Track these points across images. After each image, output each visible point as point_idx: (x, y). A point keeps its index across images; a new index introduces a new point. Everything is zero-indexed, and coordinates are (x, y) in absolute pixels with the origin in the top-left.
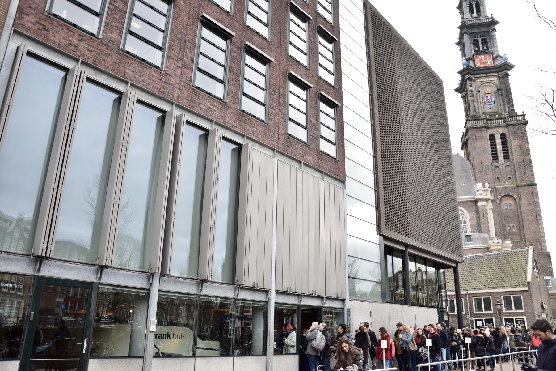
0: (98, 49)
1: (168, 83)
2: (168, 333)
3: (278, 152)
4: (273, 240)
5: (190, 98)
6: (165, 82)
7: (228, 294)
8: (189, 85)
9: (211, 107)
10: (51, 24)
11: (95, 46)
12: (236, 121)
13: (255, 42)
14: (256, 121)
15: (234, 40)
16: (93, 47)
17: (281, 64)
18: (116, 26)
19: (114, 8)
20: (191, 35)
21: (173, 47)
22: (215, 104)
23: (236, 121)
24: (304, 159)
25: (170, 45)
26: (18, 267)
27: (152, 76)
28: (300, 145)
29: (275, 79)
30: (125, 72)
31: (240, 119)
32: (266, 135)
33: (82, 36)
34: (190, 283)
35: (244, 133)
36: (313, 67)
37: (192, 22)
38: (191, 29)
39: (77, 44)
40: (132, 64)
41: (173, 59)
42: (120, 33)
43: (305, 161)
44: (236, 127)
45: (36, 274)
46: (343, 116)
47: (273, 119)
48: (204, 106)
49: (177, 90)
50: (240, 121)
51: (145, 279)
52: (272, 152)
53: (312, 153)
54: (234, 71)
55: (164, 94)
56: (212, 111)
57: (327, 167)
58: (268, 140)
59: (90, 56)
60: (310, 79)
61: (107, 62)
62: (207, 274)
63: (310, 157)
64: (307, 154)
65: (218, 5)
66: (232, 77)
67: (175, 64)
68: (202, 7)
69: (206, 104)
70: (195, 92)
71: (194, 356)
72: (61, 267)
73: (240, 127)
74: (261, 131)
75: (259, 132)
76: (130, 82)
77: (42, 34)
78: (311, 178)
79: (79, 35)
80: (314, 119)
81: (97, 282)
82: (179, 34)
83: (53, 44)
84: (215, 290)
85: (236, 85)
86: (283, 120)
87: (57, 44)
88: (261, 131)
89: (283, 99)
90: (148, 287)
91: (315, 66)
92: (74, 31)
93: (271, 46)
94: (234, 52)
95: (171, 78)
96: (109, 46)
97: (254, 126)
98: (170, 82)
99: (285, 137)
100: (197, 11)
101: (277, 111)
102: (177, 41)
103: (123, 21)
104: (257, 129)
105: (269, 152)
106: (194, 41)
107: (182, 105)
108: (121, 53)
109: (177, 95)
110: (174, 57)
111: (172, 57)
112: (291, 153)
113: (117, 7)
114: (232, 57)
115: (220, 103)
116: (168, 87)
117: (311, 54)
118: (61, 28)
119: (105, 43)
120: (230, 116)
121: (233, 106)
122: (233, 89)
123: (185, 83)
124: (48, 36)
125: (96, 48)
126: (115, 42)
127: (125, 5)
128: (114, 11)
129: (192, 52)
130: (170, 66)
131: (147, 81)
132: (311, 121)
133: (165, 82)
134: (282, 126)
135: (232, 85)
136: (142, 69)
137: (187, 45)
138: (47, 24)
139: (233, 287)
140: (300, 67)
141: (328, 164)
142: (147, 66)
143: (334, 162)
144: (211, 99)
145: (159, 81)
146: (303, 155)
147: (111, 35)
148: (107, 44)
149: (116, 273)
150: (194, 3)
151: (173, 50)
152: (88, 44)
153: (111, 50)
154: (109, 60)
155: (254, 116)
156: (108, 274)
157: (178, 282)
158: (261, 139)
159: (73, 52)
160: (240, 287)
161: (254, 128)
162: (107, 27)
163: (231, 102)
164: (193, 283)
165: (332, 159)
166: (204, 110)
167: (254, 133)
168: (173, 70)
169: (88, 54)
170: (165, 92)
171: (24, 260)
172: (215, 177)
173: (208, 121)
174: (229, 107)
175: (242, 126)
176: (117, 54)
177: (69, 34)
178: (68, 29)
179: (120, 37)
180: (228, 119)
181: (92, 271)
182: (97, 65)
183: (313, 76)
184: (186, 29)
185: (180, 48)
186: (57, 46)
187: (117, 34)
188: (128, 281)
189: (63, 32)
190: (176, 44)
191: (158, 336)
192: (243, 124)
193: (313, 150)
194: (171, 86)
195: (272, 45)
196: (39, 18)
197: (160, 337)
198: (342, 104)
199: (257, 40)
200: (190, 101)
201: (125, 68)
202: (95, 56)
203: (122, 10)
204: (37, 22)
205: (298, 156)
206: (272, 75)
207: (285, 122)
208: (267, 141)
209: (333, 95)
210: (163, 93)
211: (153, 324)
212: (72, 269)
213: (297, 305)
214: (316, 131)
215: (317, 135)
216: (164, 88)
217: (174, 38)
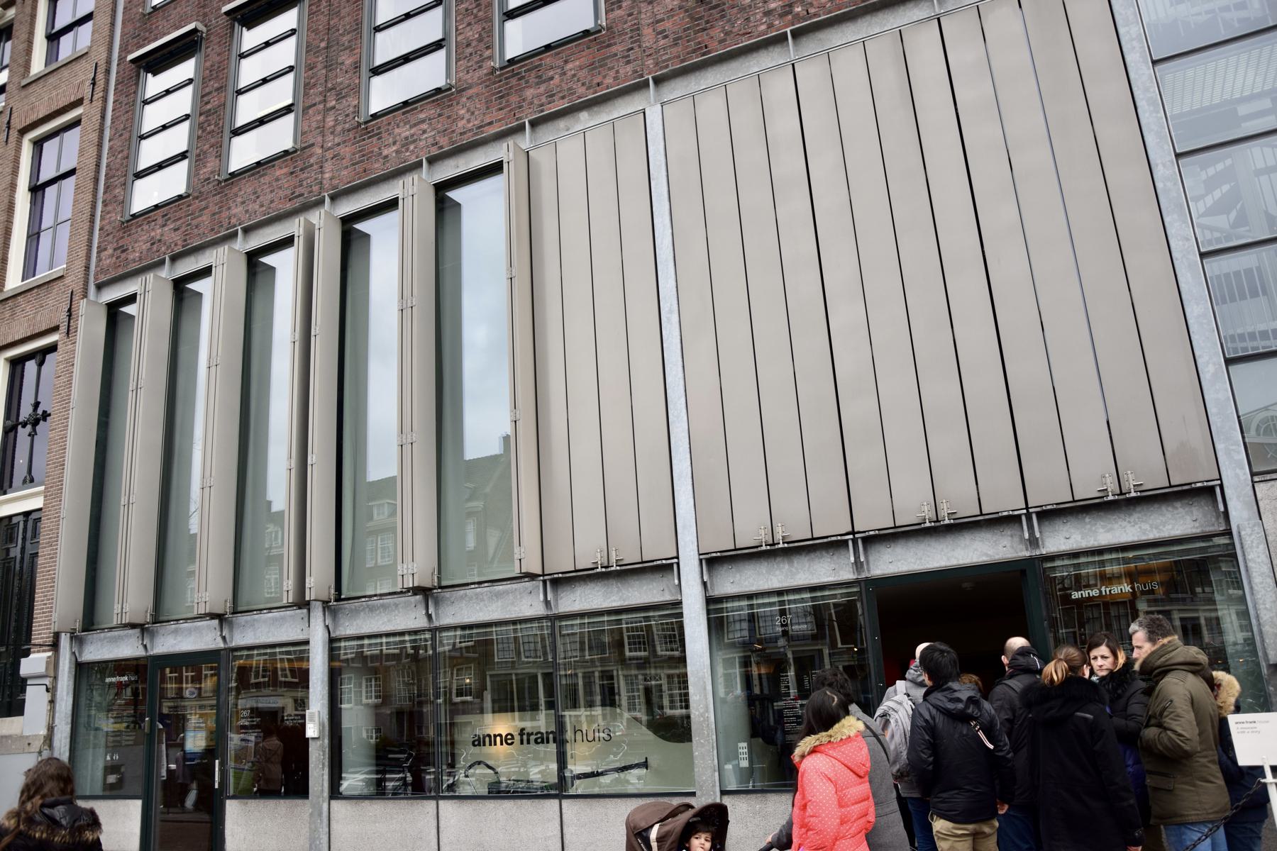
16: (180, 218)
23: (488, 108)
31: (500, 92)
35: (517, 120)
44: (491, 123)
58: (612, 73)
73: (501, 114)
74: (581, 68)
75: (574, 75)
88: (581, 68)
111: (314, 102)
133: (301, 170)
147: (205, 170)
149: (254, 620)
161: (552, 78)
180: (461, 124)
191: (533, 738)
205: (763, 27)
211: (312, 720)
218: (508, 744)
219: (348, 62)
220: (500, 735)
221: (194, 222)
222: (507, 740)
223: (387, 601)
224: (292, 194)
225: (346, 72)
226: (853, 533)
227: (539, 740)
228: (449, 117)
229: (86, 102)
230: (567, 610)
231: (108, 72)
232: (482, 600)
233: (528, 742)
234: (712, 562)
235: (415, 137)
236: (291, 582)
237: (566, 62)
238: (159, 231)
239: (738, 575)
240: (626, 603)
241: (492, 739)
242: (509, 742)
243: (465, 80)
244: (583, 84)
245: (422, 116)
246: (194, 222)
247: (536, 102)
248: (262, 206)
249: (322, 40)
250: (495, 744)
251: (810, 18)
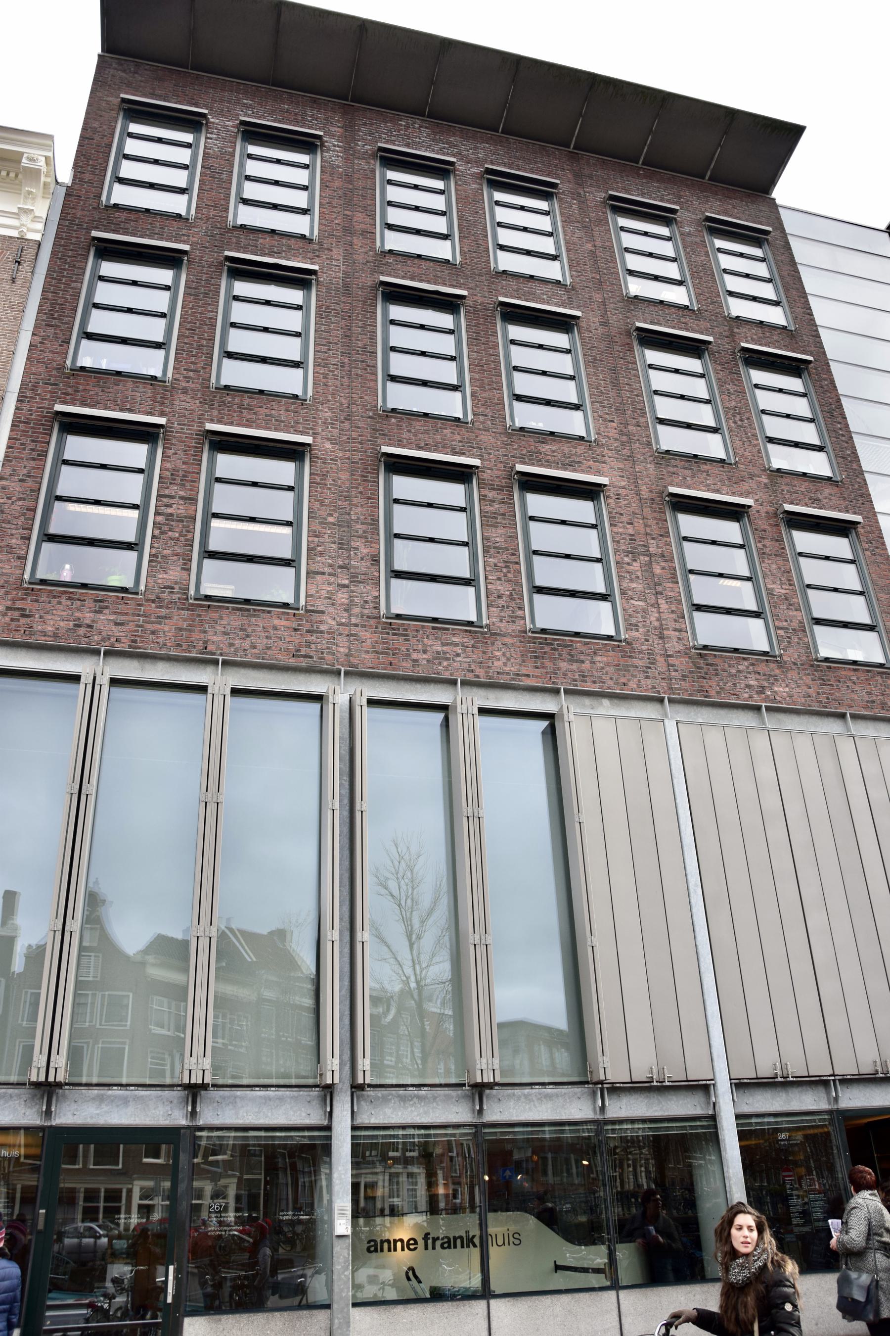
0: (139, 615)
1: (317, 632)
2: (467, 1232)
3: (671, 701)
4: (699, 938)
5: (381, 646)
6: (308, 631)
7: (573, 1111)
8: (375, 618)
9: (445, 649)
10: (37, 601)
11: (130, 612)
12: (523, 661)
13: (548, 457)
14: (588, 643)
15: (485, 475)
16: (127, 614)
17: (640, 482)
18: (173, 555)
19: (167, 520)
20: (362, 506)
21: (319, 548)
22: (456, 639)
23: (523, 661)
24: (767, 697)
25: (312, 545)
26: (7, 1113)
27: (275, 628)
28: (746, 663)
29: (628, 523)
30: (205, 642)
31: (536, 652)
32: (625, 671)
33: (101, 601)
34: (448, 1098)
35: (554, 683)
36: (747, 453)
37: (363, 476)
38: (361, 493)
39: (93, 621)
40: (221, 618)
41: (323, 573)
42: (185, 564)
43: (774, 700)
44: (528, 676)
45: (47, 1124)
46: (883, 544)
47: (639, 625)
48: (425, 652)
49: (343, 641)
50: (536, 657)
51: (316, 1103)
52: (657, 706)
53: (793, 674)
54: (498, 545)
55: (311, 657)
56: (447, 659)
57: (854, 696)
58: (636, 680)
59: (121, 634)
60: (745, 486)
61: (161, 633)
62: (478, 1067)
63: (787, 686)
64: (776, 680)
65: (426, 415)
66: (495, 561)
67: (330, 584)
68: (384, 435)
69: (428, 648)
70: (393, 629)
71: (485, 1293)
72: (101, 1099)
73: (538, 672)
74: (608, 664)
75: (603, 668)
76: (221, 658)
77: (19, 626)
78: (803, 744)
79: (95, 601)
80: (782, 584)
81: (191, 1124)
82: (331, 515)
83: (43, 638)
84: (527, 1107)
85: (510, 575)
86: (673, 616)
87: (50, 636)
89: (663, 564)
90: (326, 1123)
91: (754, 450)
92: (82, 598)
93: (599, 450)
94: (491, 501)
95: (324, 617)
96: (161, 600)
97: (582, 657)
98: (322, 627)
99: (690, 658)
100: (372, 449)
101: (651, 599)
102: (329, 532)
103: (189, 537)
104: (593, 663)
105: (649, 711)
106: (373, 516)
107: (361, 668)
108: (192, 605)
109: (347, 651)
110: (326, 570)
111: (321, 570)
112: (718, 693)
113: (172, 515)
114: (485, 516)
115: (470, 631)
116: (319, 640)
117: (735, 422)
118: (55, 601)
119: (153, 597)
120: (504, 655)
121: (511, 628)
122: (504, 588)
123: (362, 616)
124: (31, 627)
125: (133, 615)
126: (175, 586)
127: (190, 504)
128: (167, 525)
129: (371, 542)
130: (317, 592)
131: (262, 643)
132: (772, 590)
133: (308, 631)
134: (677, 633)
135: (499, 579)
136: (246, 622)
137: (357, 532)
138: (28, 605)
139: (586, 1090)
140: (704, 467)
141: (856, 688)
142: (259, 610)
143: (878, 678)
144: (440, 632)
145: (293, 633)
146: (763, 687)
147: (165, 576)
148: (158, 597)
149: (236, 1097)
150: (360, 436)
151: (321, 554)
152: (115, 613)
153: (167, 608)
154: (166, 628)
155: (577, 634)
156: (216, 1104)
157: (412, 1098)
158: (611, 683)
159: (86, 640)
160: (605, 1086)
161: (583, 662)
162: (154, 564)
163: (501, 621)
164: (458, 1095)
165: (868, 671)
166: (425, 662)
167: (583, 676)
168: (326, 598)
169: (117, 631)
170: (311, 653)
171: (19, 1096)
172: (470, 814)
173: (445, 685)
174: (499, 635)
175: (543, 668)
176: (182, 609)
177: (74, 606)
178: (70, 599)
179: (185, 573)
180: (496, 664)
181: (175, 1101)
182: (140, 648)
183: (752, 476)
184: (348, 498)
185: (339, 544)
186: (51, 639)
187: (179, 569)
188: (269, 1114)
189: (62, 608)
190: (326, 538)
191: (438, 1243)
192: (548, 663)
193: (795, 664)
194: (326, 635)
195: (603, 445)
196: (12, 599)
197: (446, 1245)
198: (872, 515)
199: (553, 451)
200: (382, 653)
201: (205, 632)
202: (135, 631)
203: (186, 517)
204: (8, 608)
205: (746, 695)
206: (618, 516)
207: (681, 620)
208: (633, 684)
209: (836, 501)
210: (306, 656)
211: (342, 1215)
212: (125, 1101)
213: (830, 1112)
214: (795, 613)
215: (800, 622)
216: (308, 644)
217: (318, 528)
218: (409, 1249)
220: (402, 1240)
222: (411, 1244)
223: (423, 1092)
224: (297, 651)
225: (362, 559)
226: (833, 1075)
227: (446, 1245)
228: (484, 653)
230: (615, 1116)
232: (531, 1101)
233: (434, 1248)
234: (740, 1086)
235: (448, 656)
236: (336, 1061)
239: (751, 1099)
240: (666, 1114)
241: (391, 1245)
242: (412, 1247)
243: (499, 627)
250: (395, 1250)
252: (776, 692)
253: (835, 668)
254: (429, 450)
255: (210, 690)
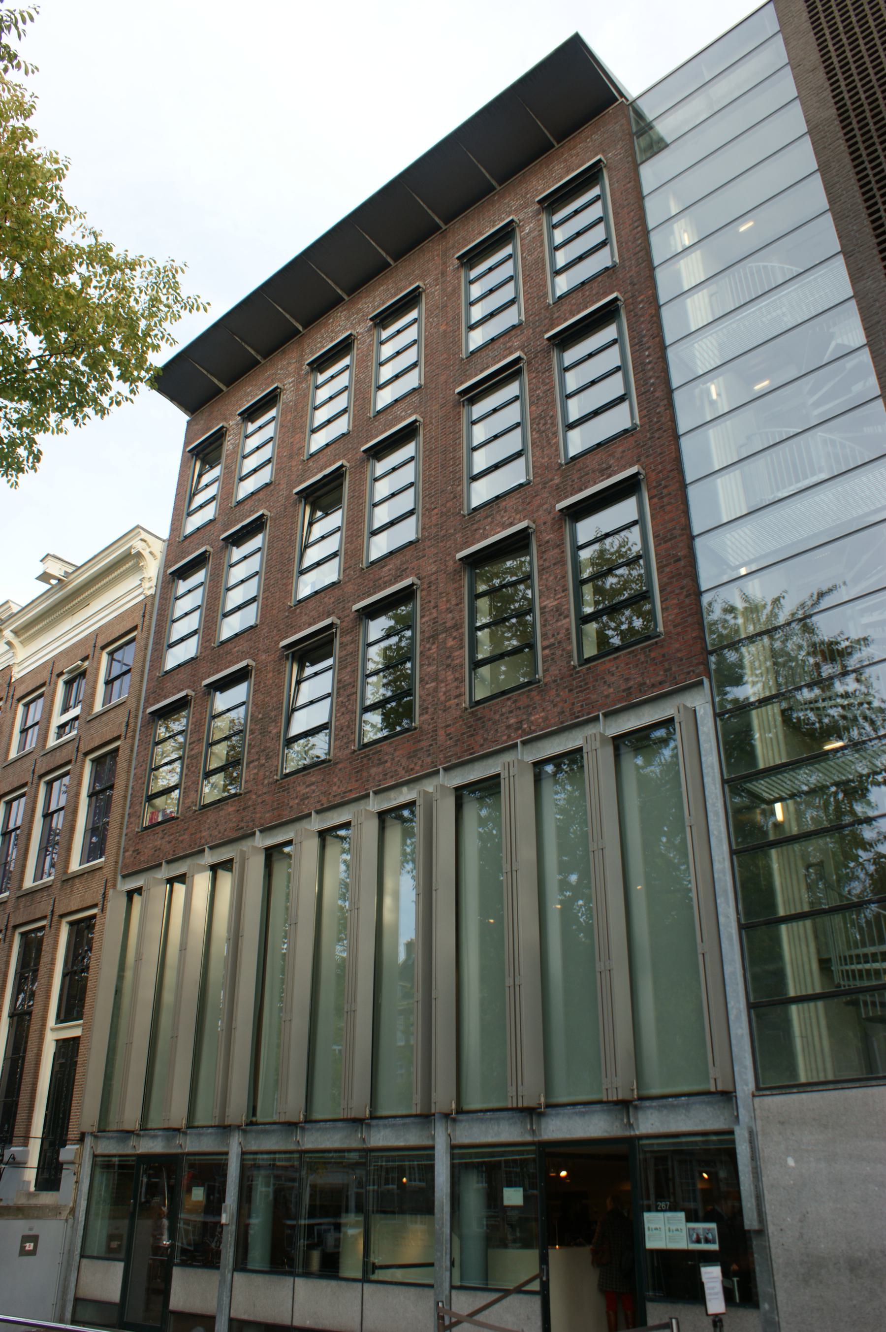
28: (509, 703)
133: (244, 809)
161: (386, 762)
180: (335, 788)
205: (505, 738)
219: (274, 731)
221: (180, 839)
229: (123, 738)
231: (136, 717)
237: (395, 750)
238: (159, 842)
244: (404, 768)
245: (313, 779)
246: (180, 839)
247: (377, 778)
248: (219, 833)
249: (260, 713)
251: (531, 733)
252: (532, 722)
253: (594, 666)
254: (396, 582)
255: (676, 720)
